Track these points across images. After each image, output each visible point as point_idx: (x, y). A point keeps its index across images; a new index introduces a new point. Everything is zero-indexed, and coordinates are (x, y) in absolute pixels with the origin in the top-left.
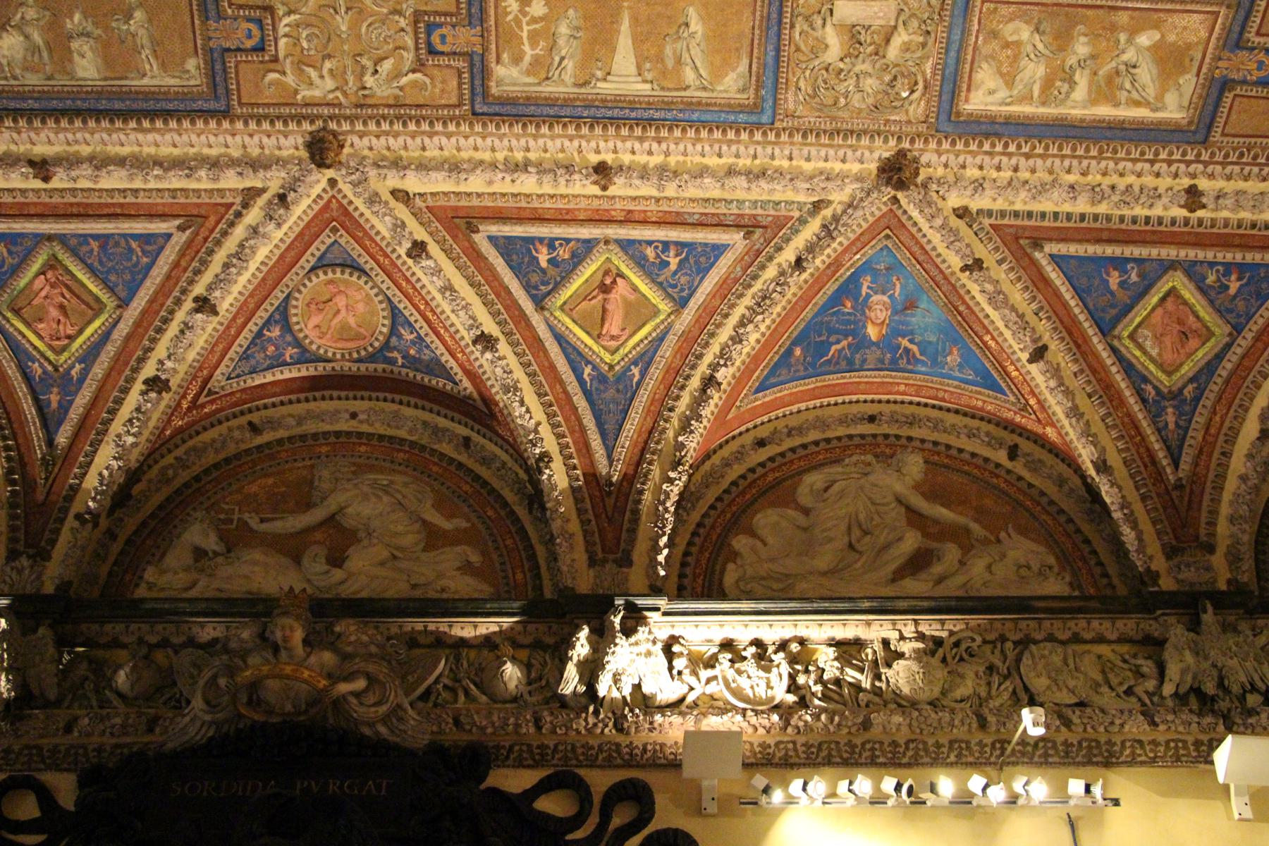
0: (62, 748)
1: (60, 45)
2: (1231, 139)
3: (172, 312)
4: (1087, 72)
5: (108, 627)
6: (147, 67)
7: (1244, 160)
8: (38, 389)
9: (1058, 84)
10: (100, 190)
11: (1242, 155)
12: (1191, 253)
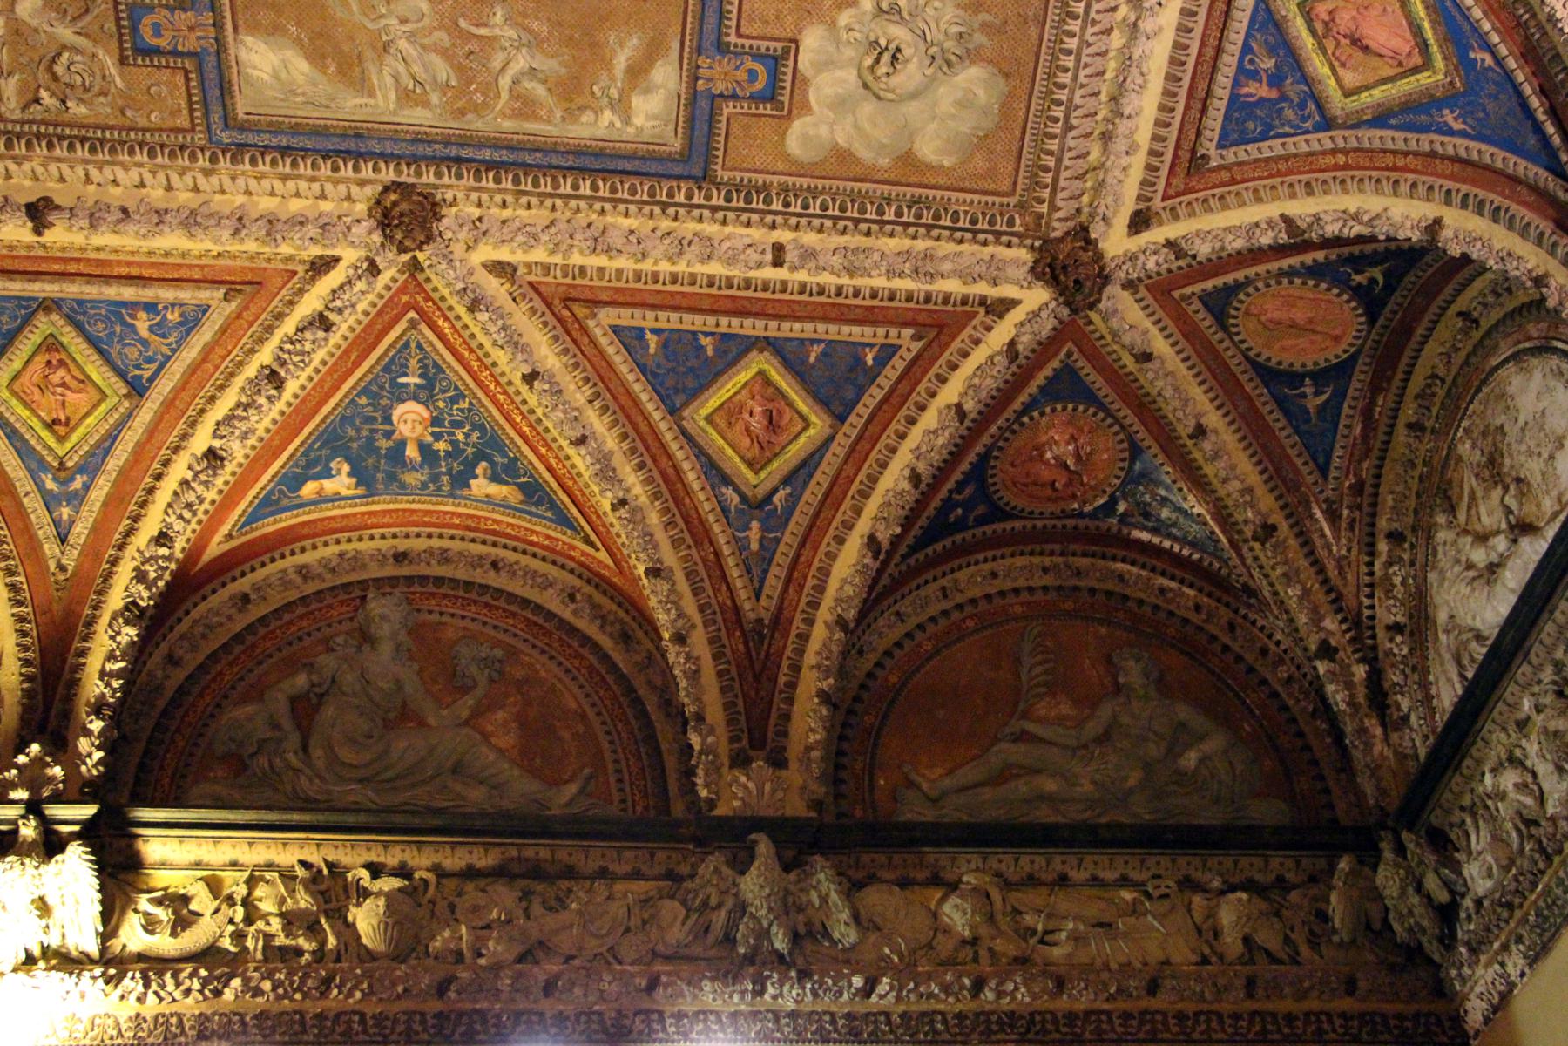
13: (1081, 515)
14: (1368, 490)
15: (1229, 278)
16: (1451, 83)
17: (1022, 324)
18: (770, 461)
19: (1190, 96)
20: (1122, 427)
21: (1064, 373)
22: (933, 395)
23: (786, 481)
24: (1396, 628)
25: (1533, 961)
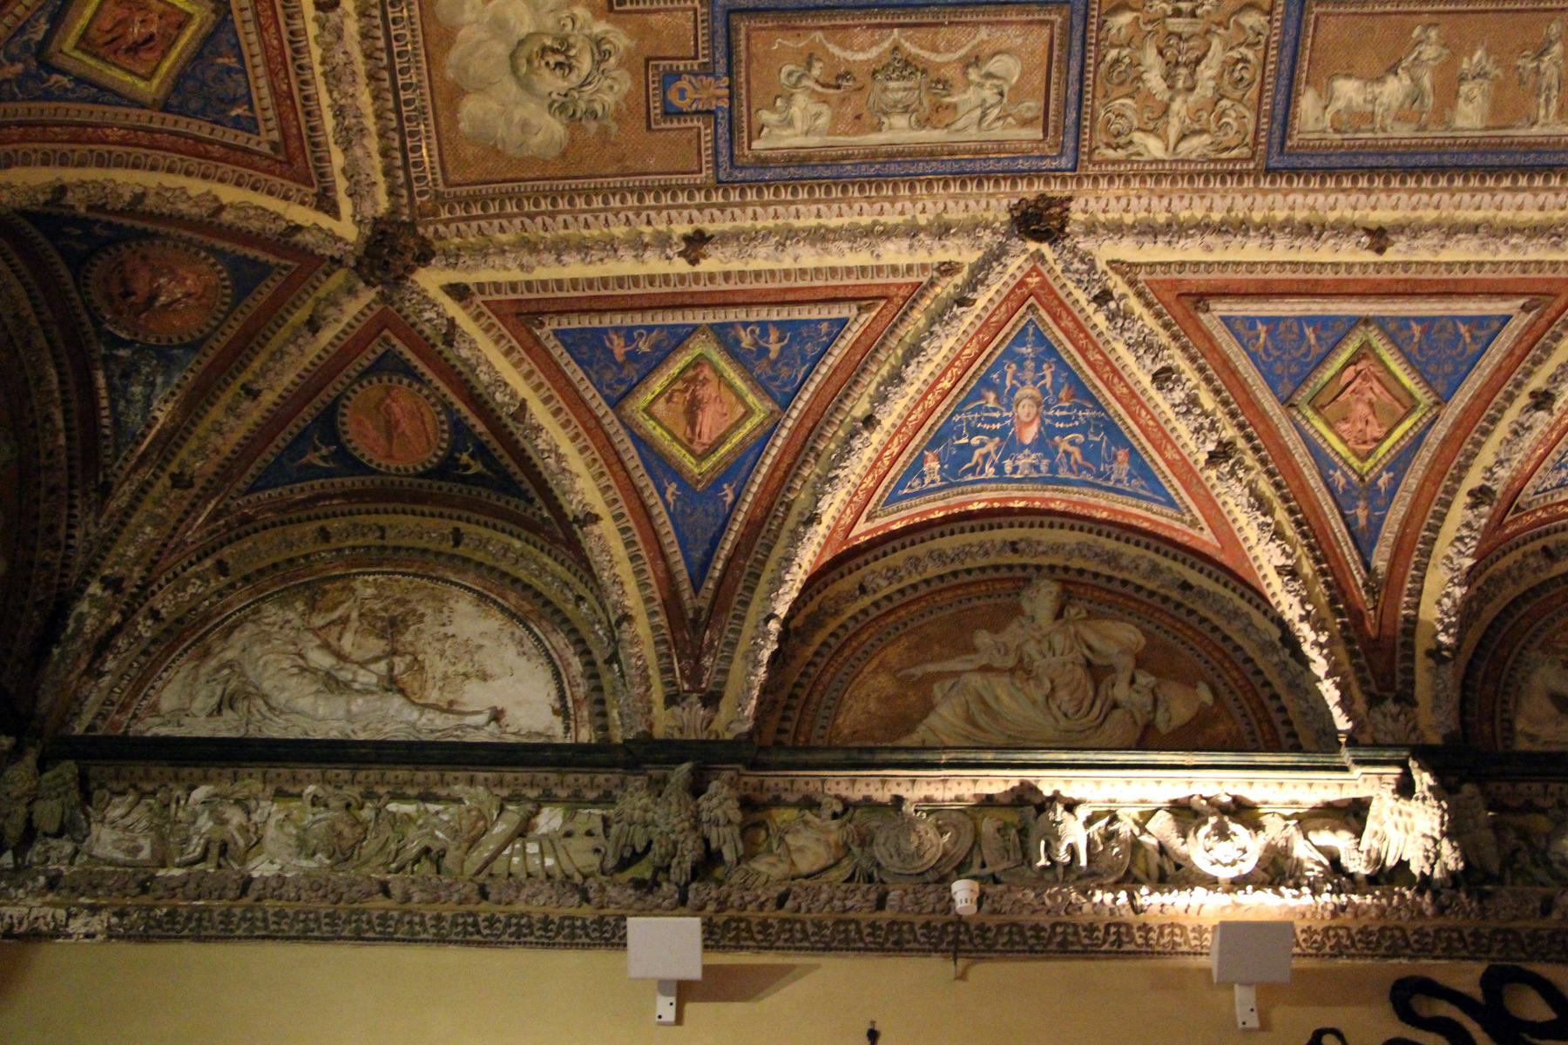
0: (1545, 934)
1: (1449, 87)
3: (1501, 410)
5: (1522, 787)
6: (1542, 112)
8: (1342, 503)
10: (1438, 264)
13: (97, 323)
14: (248, 527)
15: (422, 367)
16: (698, 482)
17: (320, 229)
18: (95, 56)
19: (591, 298)
20: (216, 328)
21: (271, 272)
22: (222, 180)
23: (80, 80)
24: (155, 615)
25: (111, 934)
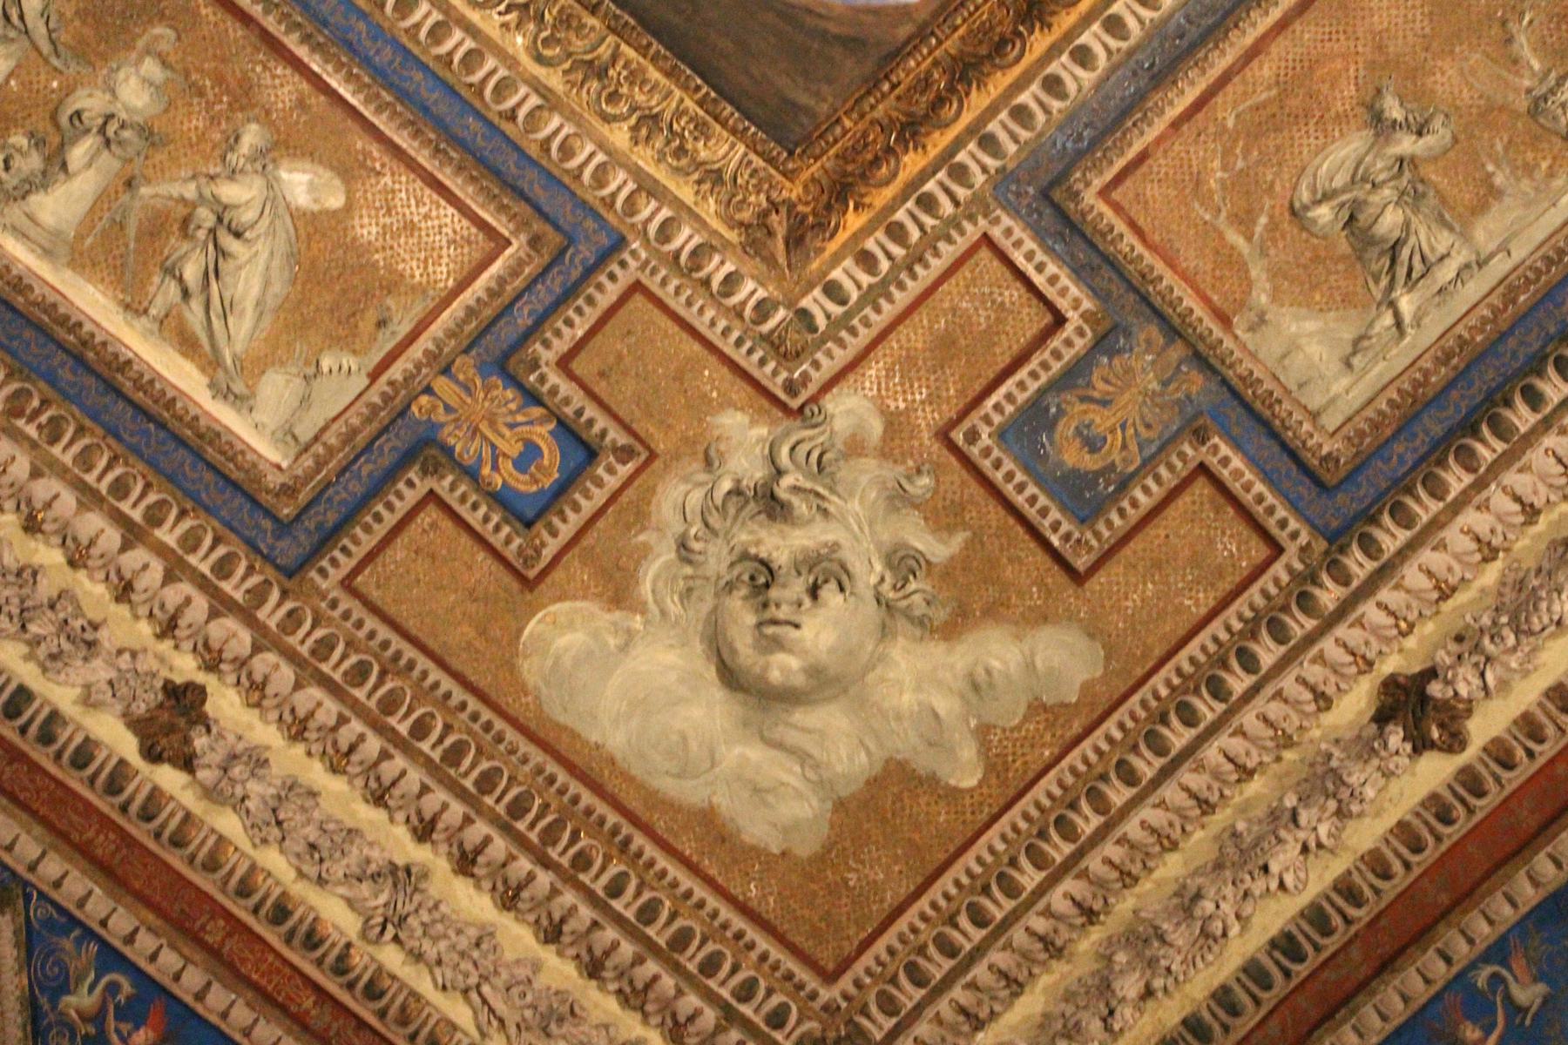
2: (358, 611)
4: (109, 162)
7: (360, 694)
9: (19, 140)
11: (359, 674)
12: (77, 886)
